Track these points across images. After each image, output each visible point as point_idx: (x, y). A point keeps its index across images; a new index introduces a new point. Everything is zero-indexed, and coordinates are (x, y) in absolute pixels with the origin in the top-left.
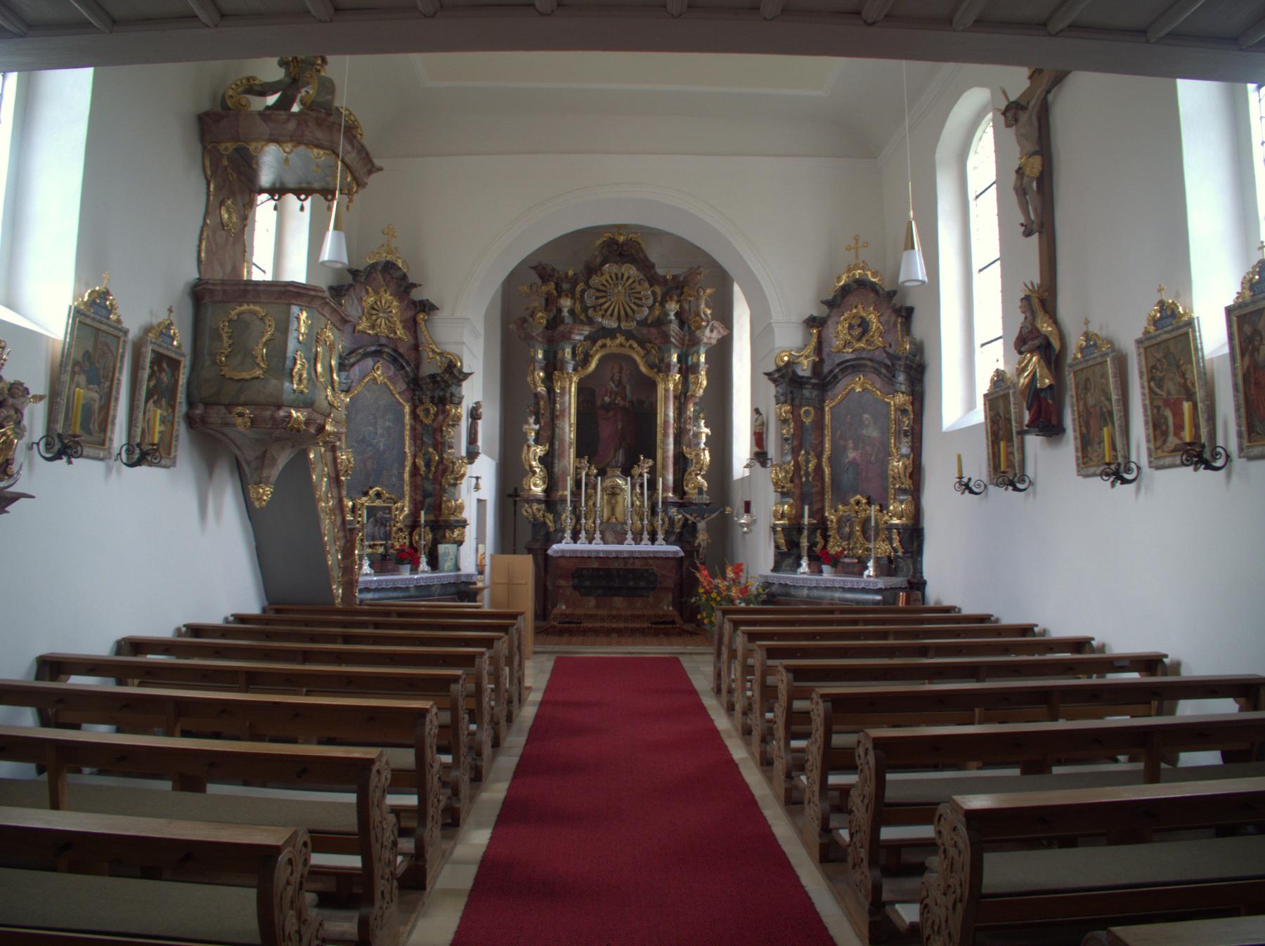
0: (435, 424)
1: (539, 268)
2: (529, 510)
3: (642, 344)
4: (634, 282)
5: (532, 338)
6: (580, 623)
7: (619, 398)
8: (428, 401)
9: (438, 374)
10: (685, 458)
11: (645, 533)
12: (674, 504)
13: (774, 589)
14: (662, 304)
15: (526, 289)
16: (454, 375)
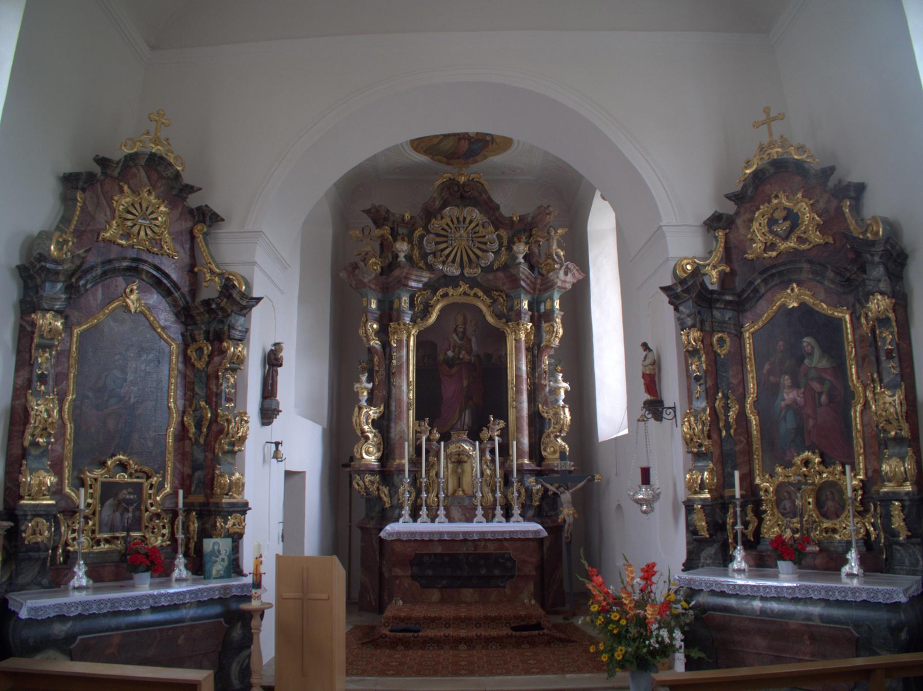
0: (210, 368)
1: (373, 211)
2: (361, 483)
3: (487, 292)
4: (477, 225)
5: (364, 285)
6: (419, 631)
7: (463, 352)
8: (202, 337)
9: (213, 300)
10: (542, 418)
11: (498, 508)
12: (532, 472)
13: (701, 599)
14: (509, 249)
15: (358, 233)
16: (234, 300)
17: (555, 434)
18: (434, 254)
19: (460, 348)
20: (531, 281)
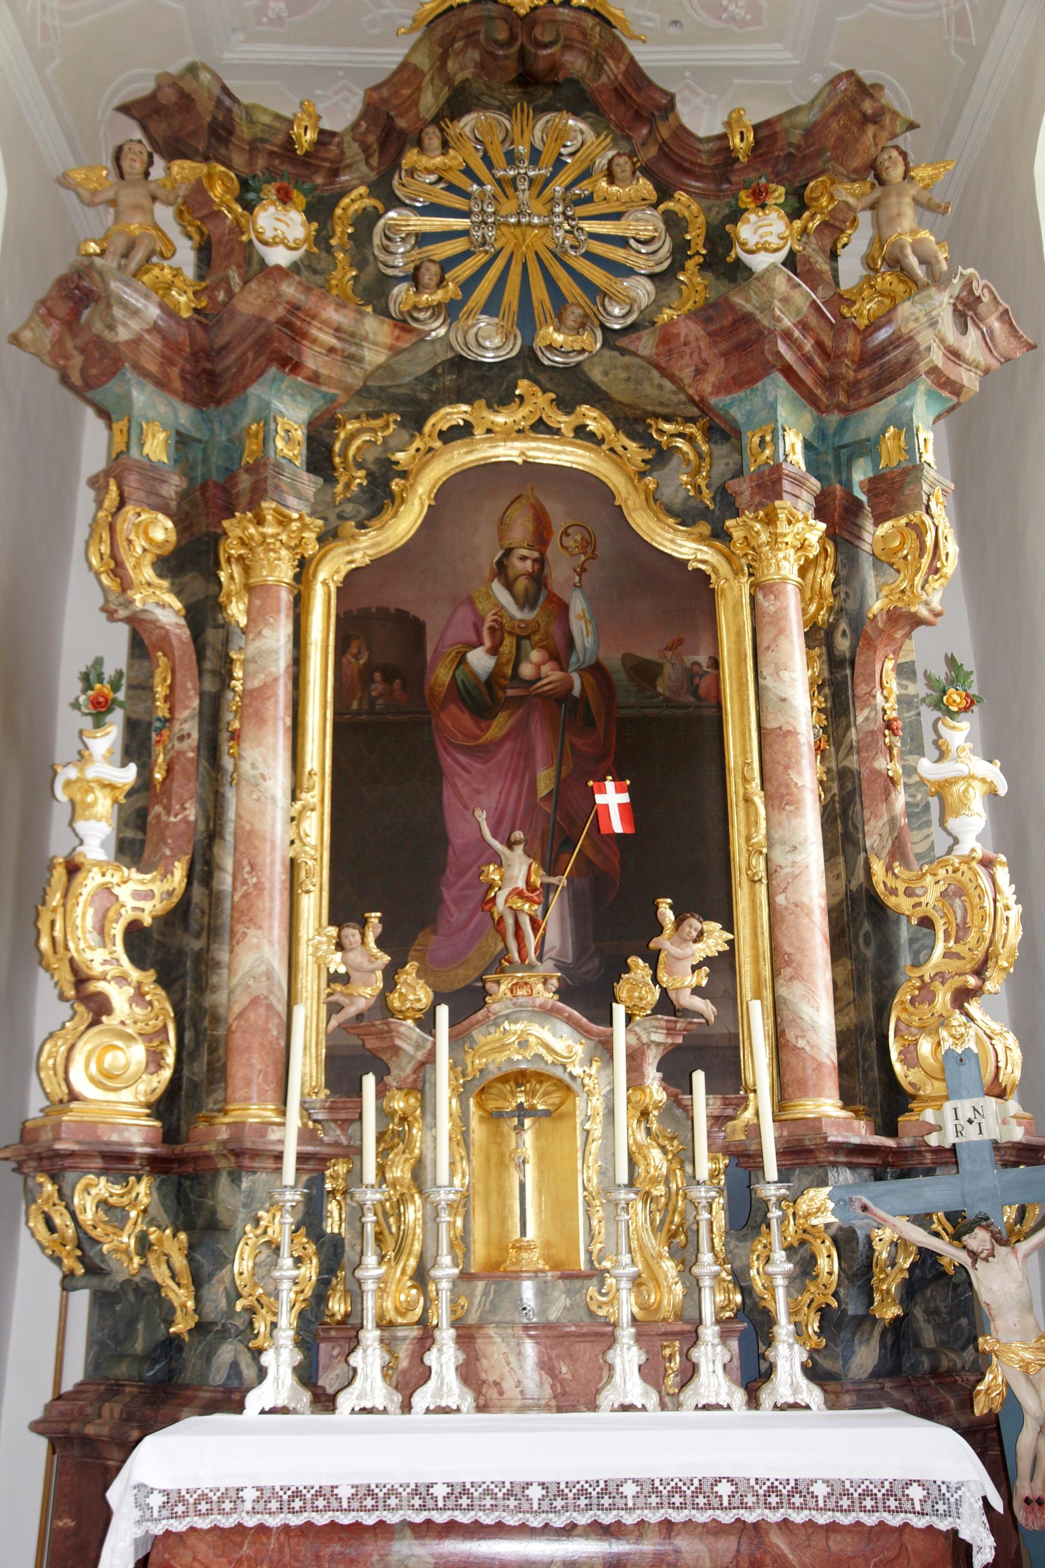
4: (586, 174)
7: (536, 655)
11: (709, 1332)
17: (956, 982)
18: (415, 278)
19: (519, 639)
20: (819, 344)
